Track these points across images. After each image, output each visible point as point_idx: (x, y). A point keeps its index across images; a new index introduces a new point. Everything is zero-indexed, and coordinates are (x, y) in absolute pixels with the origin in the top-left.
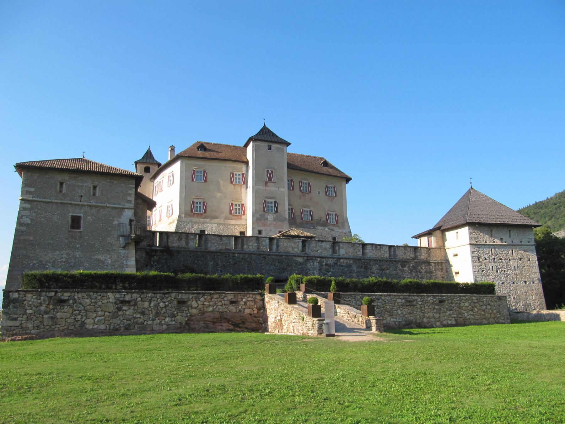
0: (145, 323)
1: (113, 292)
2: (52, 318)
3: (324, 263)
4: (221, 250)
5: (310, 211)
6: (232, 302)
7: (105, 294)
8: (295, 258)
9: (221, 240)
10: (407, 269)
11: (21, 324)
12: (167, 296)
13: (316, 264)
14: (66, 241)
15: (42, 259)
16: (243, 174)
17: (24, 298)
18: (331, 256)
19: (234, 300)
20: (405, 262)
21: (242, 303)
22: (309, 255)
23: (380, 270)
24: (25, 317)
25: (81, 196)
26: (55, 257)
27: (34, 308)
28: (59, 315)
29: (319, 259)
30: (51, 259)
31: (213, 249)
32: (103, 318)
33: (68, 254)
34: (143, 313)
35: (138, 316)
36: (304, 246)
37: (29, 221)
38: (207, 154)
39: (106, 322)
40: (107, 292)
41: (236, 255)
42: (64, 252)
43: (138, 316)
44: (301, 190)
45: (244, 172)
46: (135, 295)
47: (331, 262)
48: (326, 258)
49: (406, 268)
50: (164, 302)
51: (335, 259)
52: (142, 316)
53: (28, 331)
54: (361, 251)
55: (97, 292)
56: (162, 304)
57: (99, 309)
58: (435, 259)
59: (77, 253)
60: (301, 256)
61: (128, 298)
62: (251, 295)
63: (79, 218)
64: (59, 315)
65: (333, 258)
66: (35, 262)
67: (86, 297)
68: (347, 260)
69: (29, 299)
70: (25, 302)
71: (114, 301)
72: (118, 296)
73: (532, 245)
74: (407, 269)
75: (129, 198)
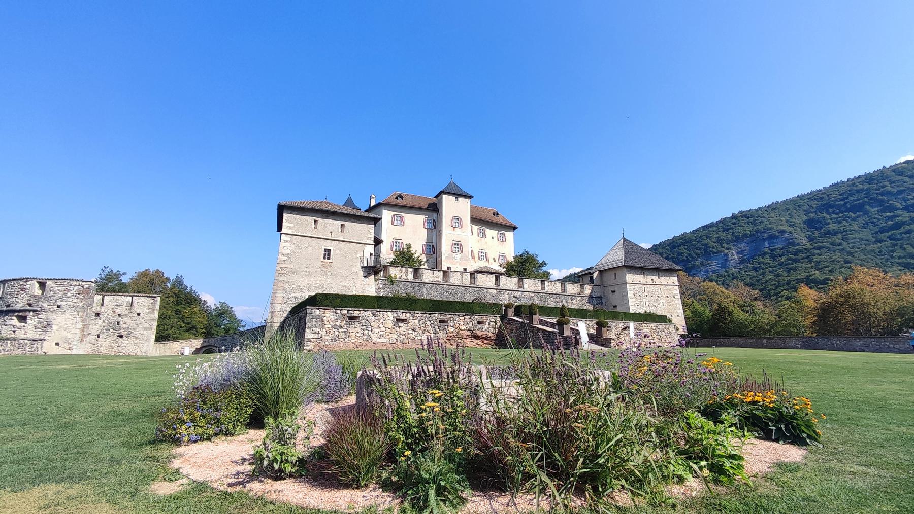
0: (416, 338)
1: (391, 312)
2: (345, 332)
3: (512, 295)
4: (432, 281)
5: (486, 253)
6: (479, 323)
7: (386, 313)
8: (489, 290)
9: (433, 273)
10: (575, 302)
11: (322, 337)
12: (432, 315)
13: (506, 296)
14: (320, 269)
15: (299, 284)
16: (434, 221)
17: (324, 315)
18: (517, 290)
19: (481, 321)
20: (573, 296)
21: (487, 324)
22: (501, 288)
23: (555, 302)
24: (324, 330)
25: (331, 233)
26: (310, 282)
27: (331, 324)
28: (351, 330)
29: (508, 292)
30: (308, 284)
31: (426, 281)
32: (384, 332)
33: (321, 281)
34: (414, 330)
35: (411, 332)
36: (496, 280)
37: (289, 252)
38: (404, 202)
39: (387, 336)
40: (387, 312)
41: (445, 286)
42: (319, 279)
43: (411, 332)
44: (478, 236)
45: (435, 219)
46: (408, 315)
47: (517, 294)
48: (513, 291)
49: (574, 301)
50: (430, 321)
51: (520, 292)
52: (414, 333)
53: (327, 343)
54: (540, 285)
55: (379, 312)
56: (429, 323)
57: (381, 325)
58: (596, 294)
59: (329, 280)
60: (495, 289)
61: (401, 318)
62: (493, 317)
63: (329, 251)
64: (351, 330)
65: (519, 291)
66: (293, 286)
67: (372, 315)
68: (530, 293)
69: (327, 315)
70: (324, 318)
71: (393, 319)
72: (395, 314)
73: (677, 286)
74: (575, 302)
75: (370, 236)
